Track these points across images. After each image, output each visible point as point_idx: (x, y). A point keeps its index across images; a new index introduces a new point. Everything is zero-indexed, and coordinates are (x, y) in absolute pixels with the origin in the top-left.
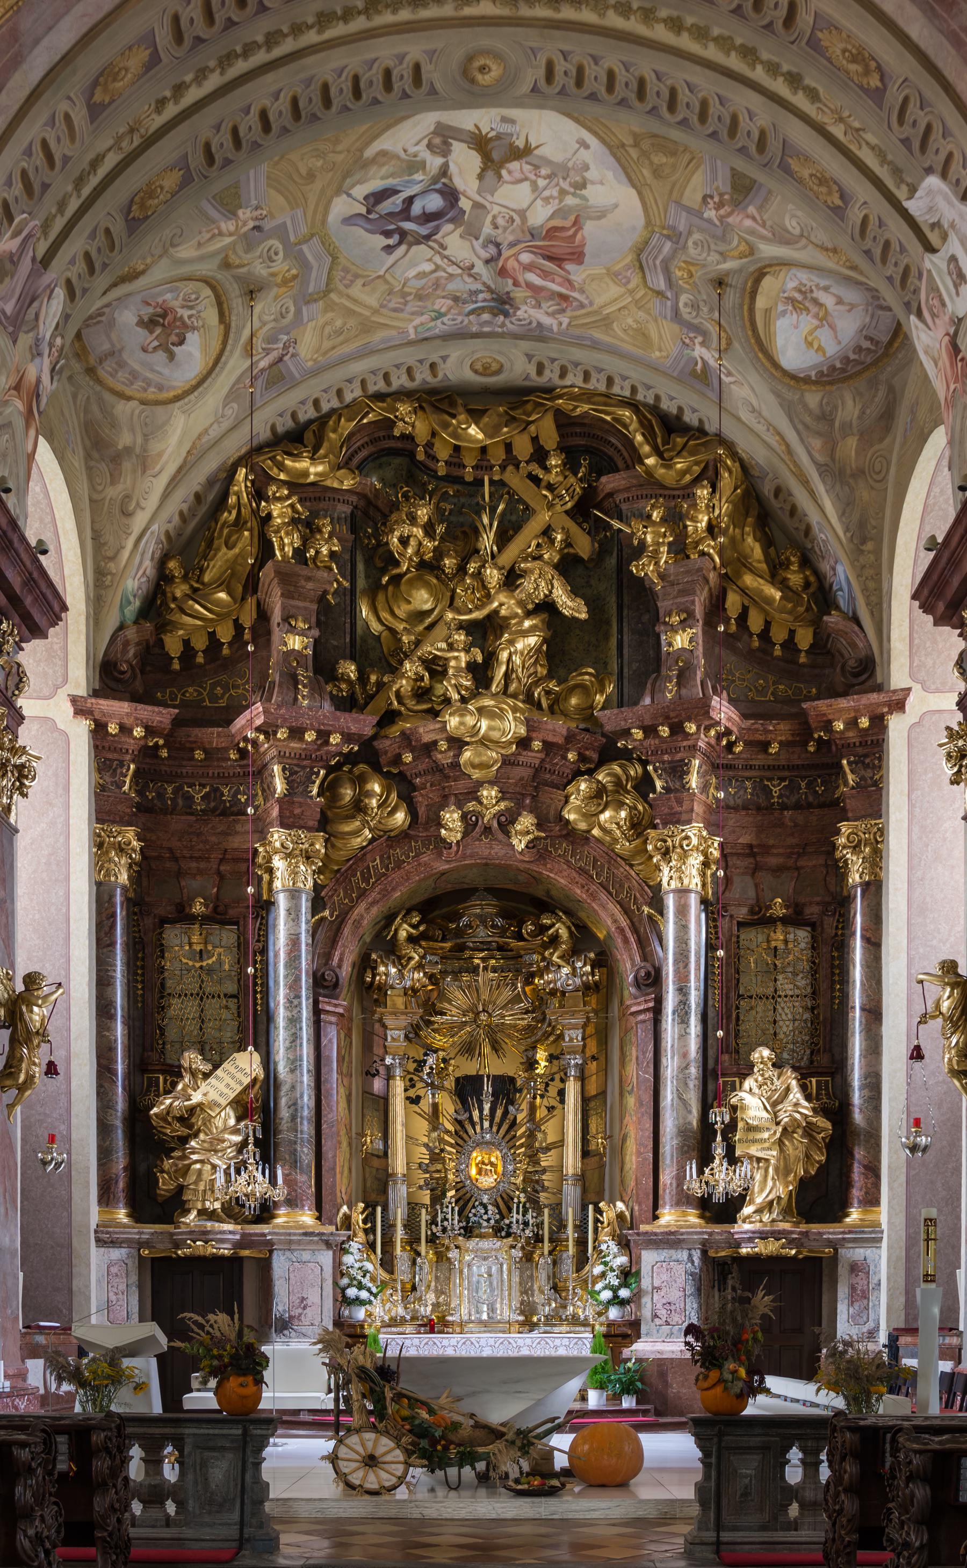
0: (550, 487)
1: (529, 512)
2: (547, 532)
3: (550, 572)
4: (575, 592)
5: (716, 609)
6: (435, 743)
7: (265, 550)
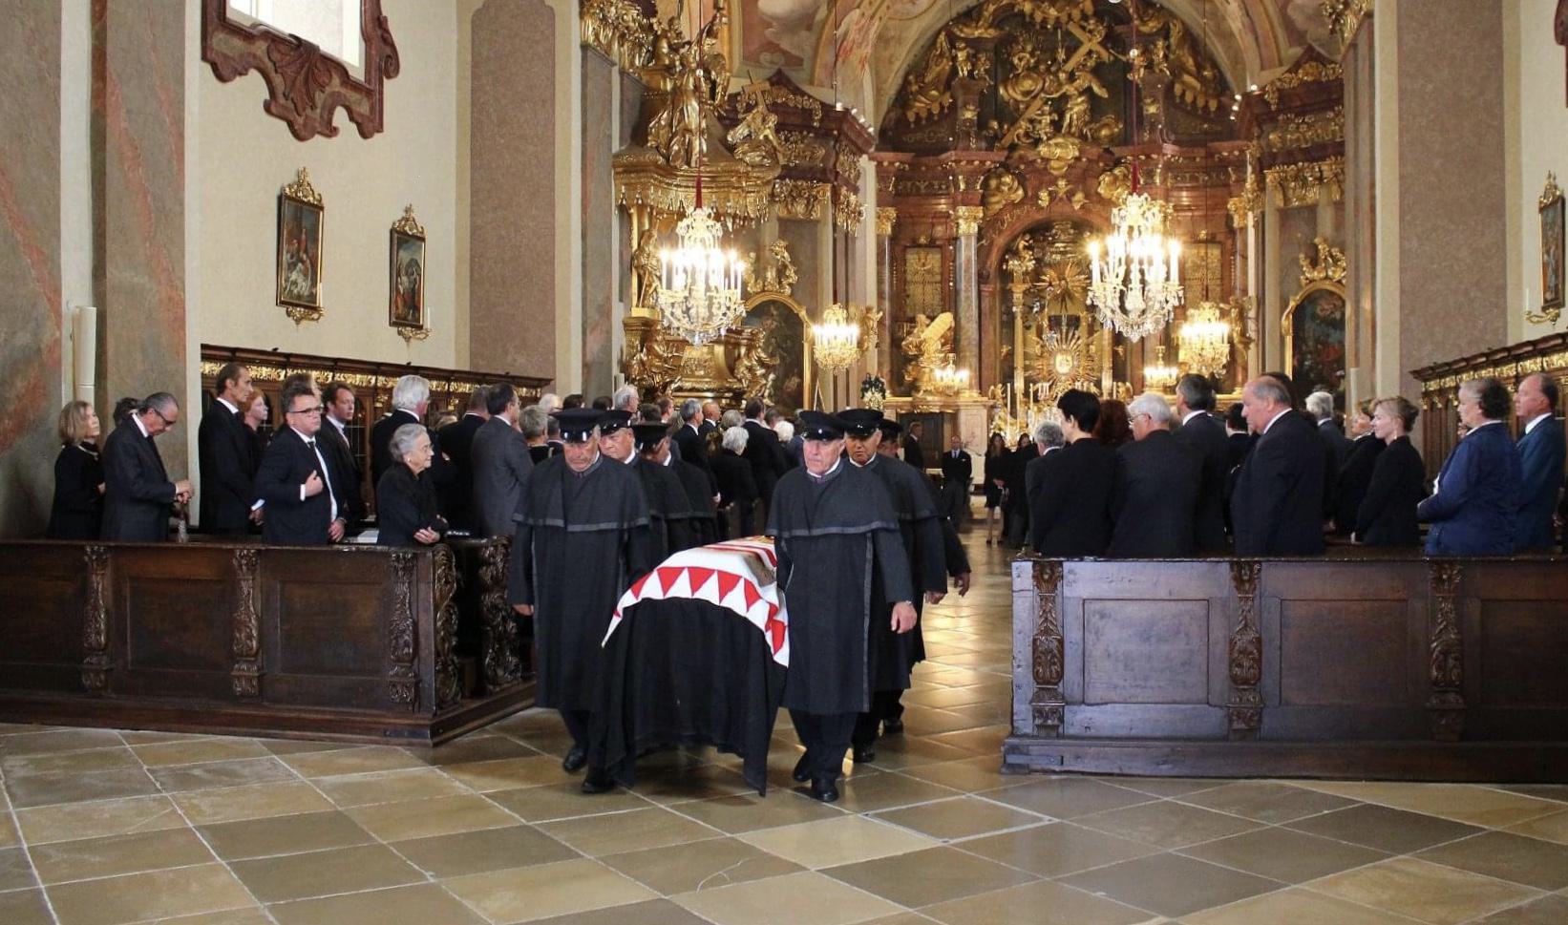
0: (1090, 32)
1: (1079, 44)
2: (1090, 53)
3: (1089, 76)
4: (1103, 86)
5: (1169, 89)
6: (1035, 161)
7: (954, 71)
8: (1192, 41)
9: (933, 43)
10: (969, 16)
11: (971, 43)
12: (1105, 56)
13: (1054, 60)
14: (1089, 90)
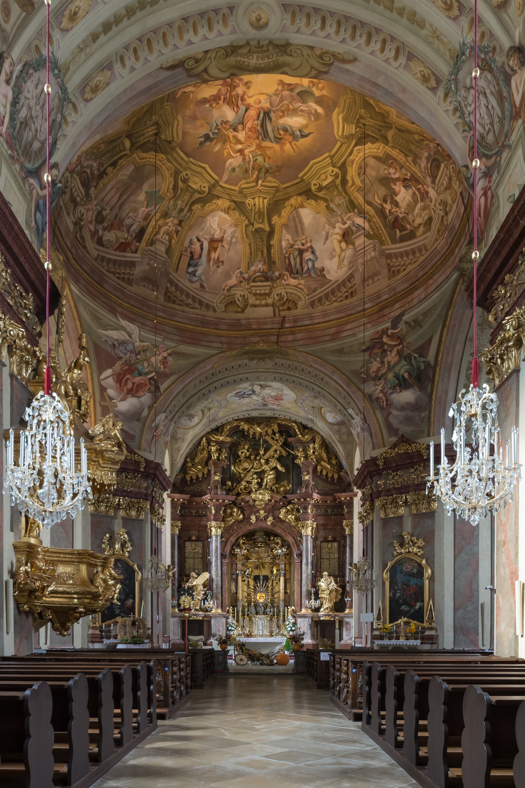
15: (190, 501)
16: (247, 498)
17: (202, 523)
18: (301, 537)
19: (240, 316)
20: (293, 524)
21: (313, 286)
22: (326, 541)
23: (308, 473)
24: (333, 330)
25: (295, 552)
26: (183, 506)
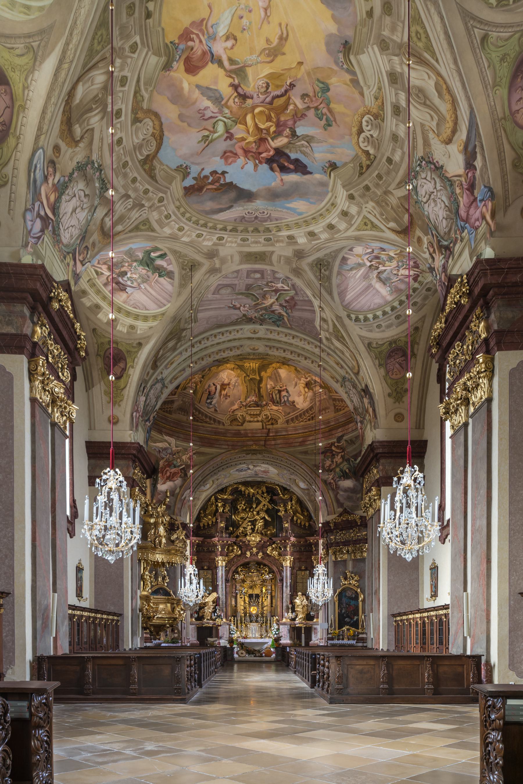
2: (264, 505)
4: (269, 517)
7: (217, 510)
8: (300, 502)
9: (209, 499)
10: (223, 491)
11: (223, 500)
12: (270, 507)
13: (252, 507)
14: (264, 517)
15: (203, 542)
16: (244, 540)
17: (212, 557)
18: (282, 567)
19: (241, 428)
20: (277, 557)
21: (288, 411)
22: (300, 569)
23: (287, 522)
24: (301, 439)
25: (278, 577)
26: (198, 545)
